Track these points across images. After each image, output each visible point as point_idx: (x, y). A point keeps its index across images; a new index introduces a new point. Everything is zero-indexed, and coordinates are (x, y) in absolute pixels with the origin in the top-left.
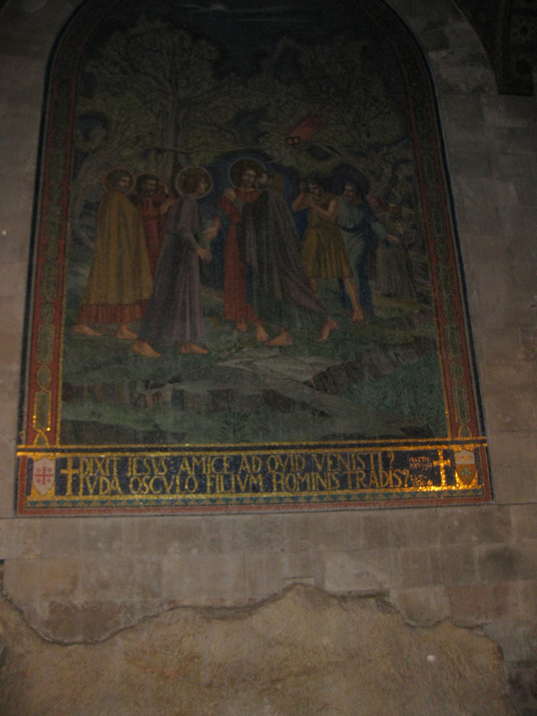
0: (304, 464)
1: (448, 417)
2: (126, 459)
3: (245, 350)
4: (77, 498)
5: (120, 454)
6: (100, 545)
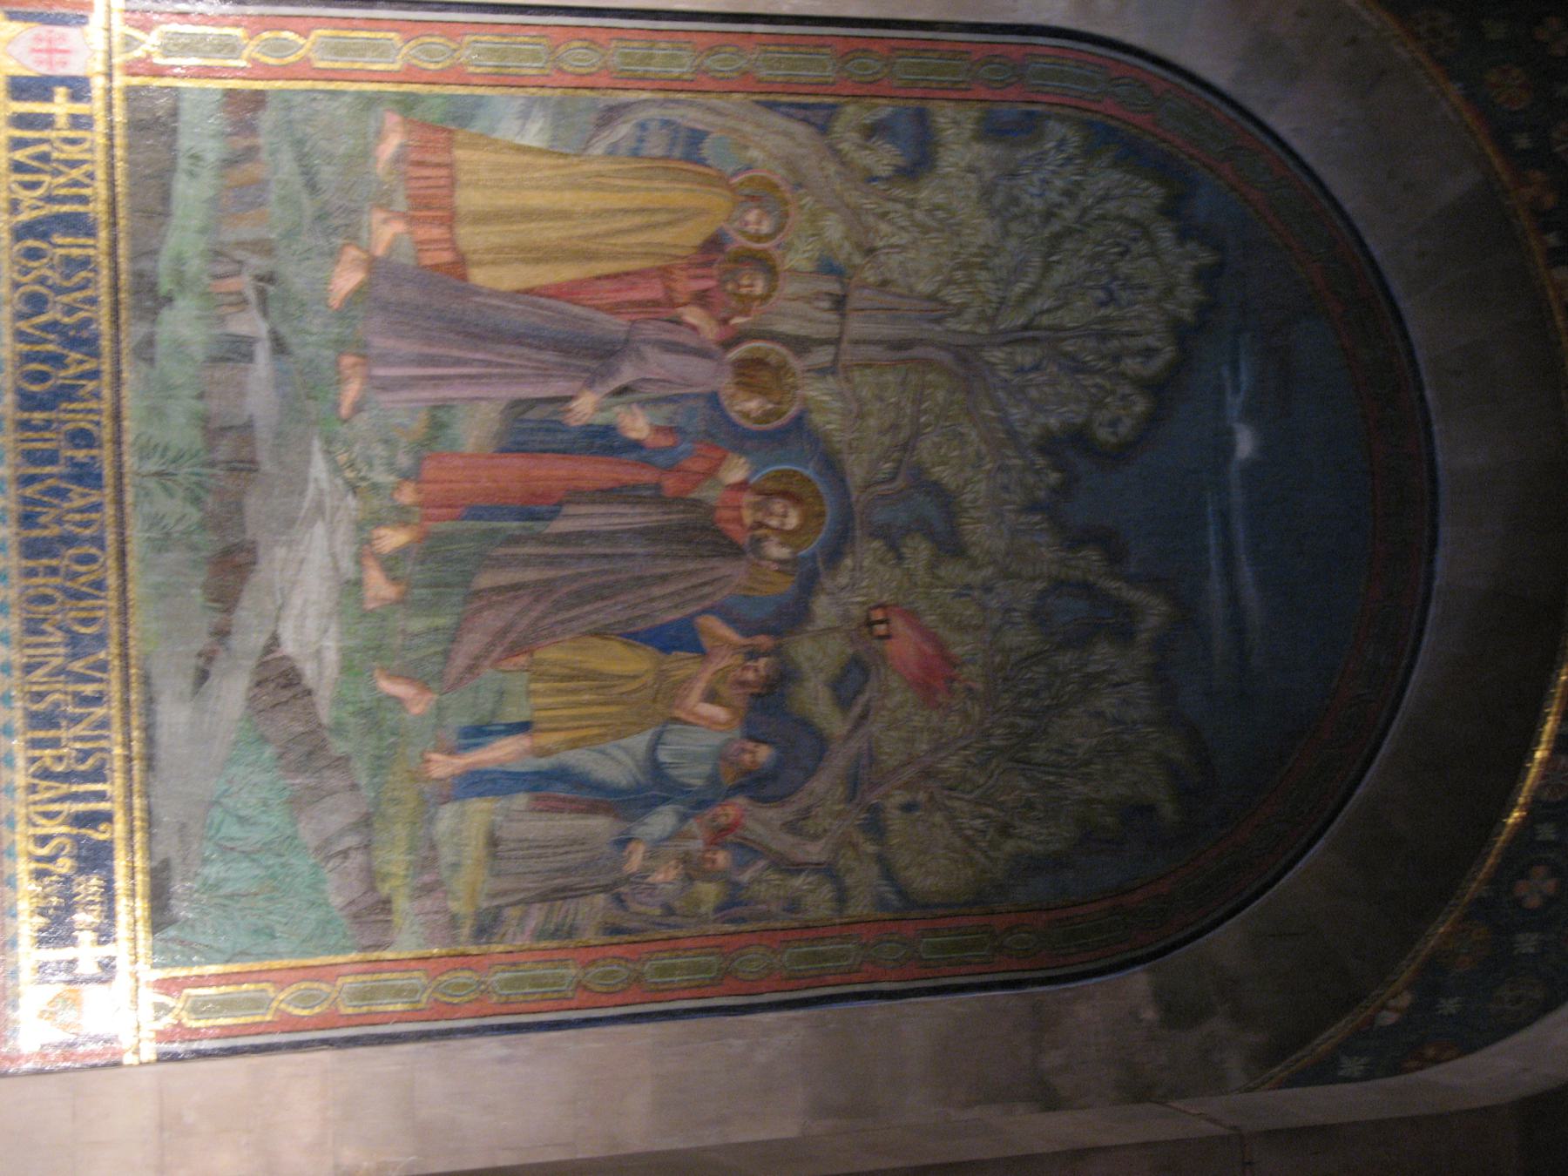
0: (83, 630)
2: (91, 232)
3: (350, 497)
5: (103, 217)
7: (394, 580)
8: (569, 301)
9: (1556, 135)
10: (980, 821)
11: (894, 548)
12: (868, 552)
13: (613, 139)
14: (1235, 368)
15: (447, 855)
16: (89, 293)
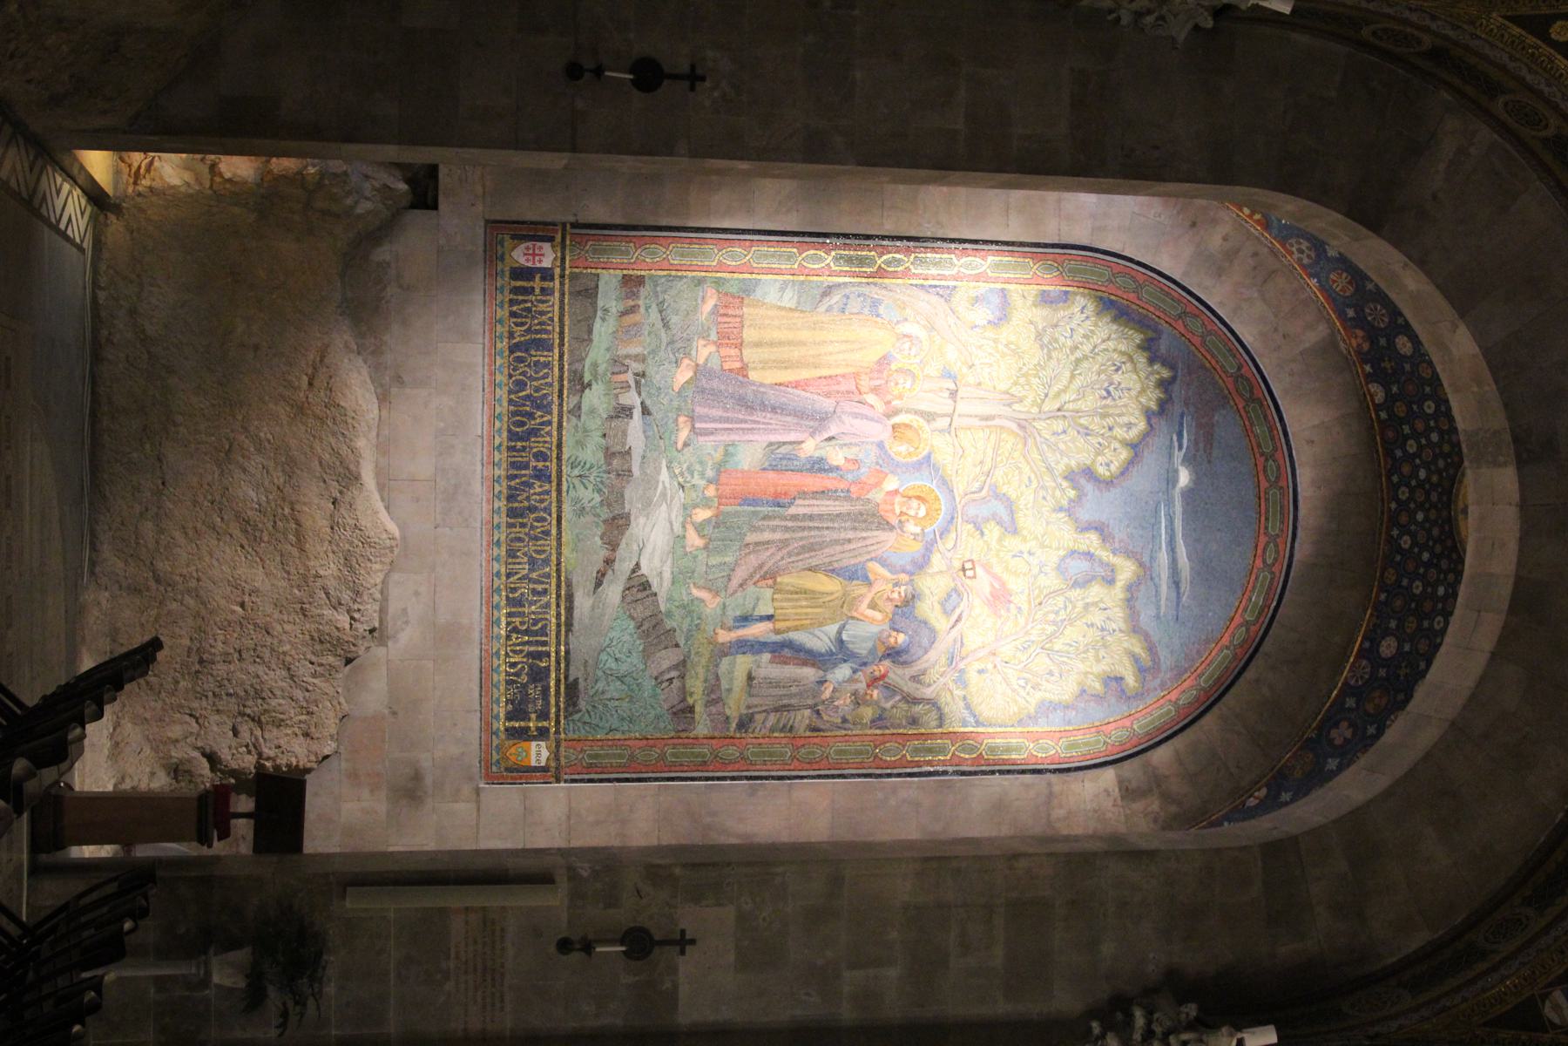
0: (538, 557)
7: (703, 536)
9: (1367, 311)
11: (978, 528)
15: (724, 685)
16: (547, 380)
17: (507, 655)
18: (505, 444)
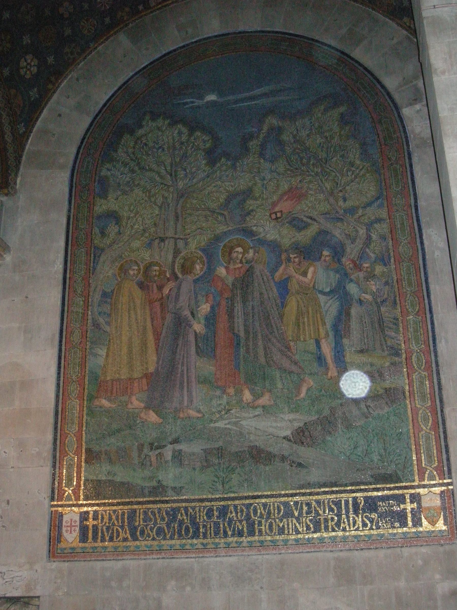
0: (282, 511)
1: (415, 462)
3: (231, 411)
4: (96, 545)
6: (113, 584)
7: (262, 395)
8: (160, 335)
10: (349, 173)
11: (249, 213)
12: (251, 222)
13: (104, 323)
14: (186, 103)
17: (357, 529)
18: (201, 540)
